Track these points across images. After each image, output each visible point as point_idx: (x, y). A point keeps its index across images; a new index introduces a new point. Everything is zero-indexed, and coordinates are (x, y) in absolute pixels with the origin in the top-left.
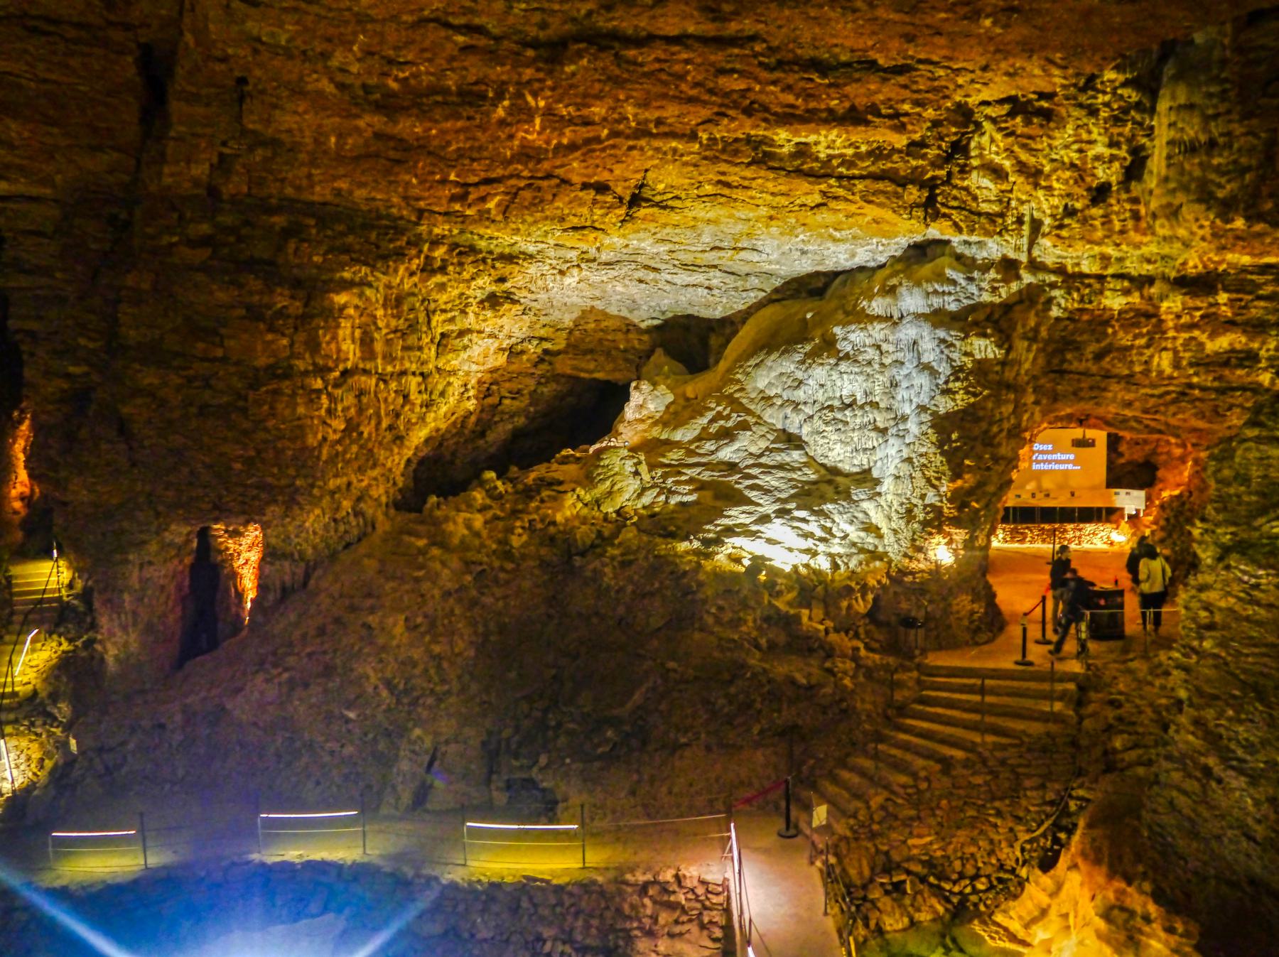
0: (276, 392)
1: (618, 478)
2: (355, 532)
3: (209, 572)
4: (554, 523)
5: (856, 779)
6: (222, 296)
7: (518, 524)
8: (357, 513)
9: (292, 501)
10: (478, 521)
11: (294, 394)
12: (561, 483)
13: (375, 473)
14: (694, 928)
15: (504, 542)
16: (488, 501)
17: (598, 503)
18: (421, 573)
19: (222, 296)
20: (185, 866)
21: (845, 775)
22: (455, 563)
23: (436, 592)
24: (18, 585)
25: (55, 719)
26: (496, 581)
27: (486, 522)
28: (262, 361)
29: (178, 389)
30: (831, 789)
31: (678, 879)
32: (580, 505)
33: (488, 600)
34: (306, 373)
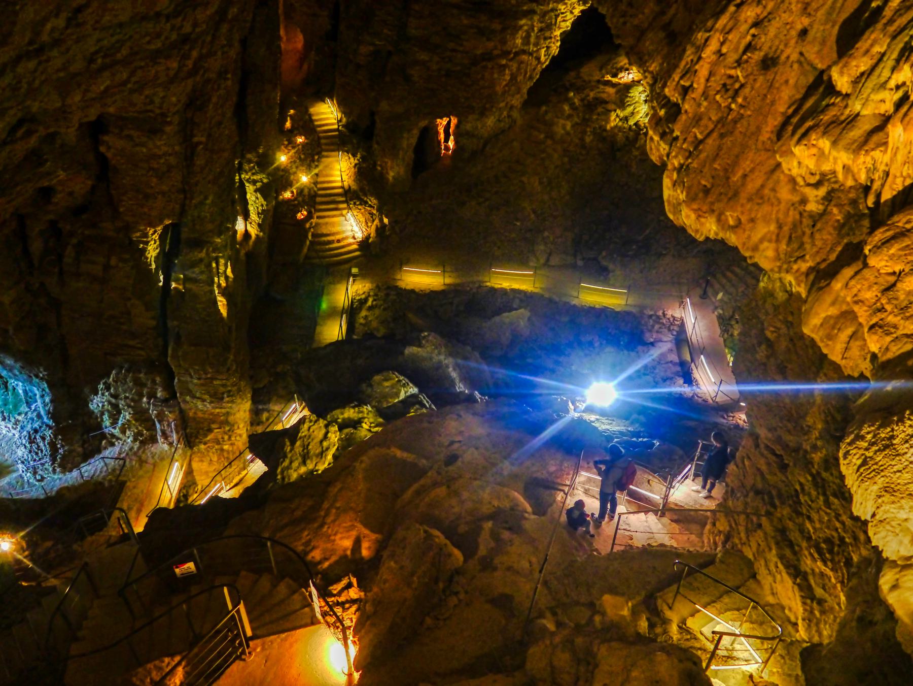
0: (485, 67)
1: (637, 105)
2: (507, 126)
3: (428, 133)
4: (605, 130)
6: (465, 22)
7: (588, 129)
9: (483, 113)
11: (493, 68)
12: (607, 103)
13: (519, 96)
14: (666, 330)
16: (571, 112)
17: (626, 119)
18: (543, 155)
19: (465, 22)
20: (458, 285)
21: (729, 274)
23: (553, 167)
24: (317, 120)
25: (366, 203)
27: (573, 126)
28: (479, 52)
31: (664, 315)
32: (618, 120)
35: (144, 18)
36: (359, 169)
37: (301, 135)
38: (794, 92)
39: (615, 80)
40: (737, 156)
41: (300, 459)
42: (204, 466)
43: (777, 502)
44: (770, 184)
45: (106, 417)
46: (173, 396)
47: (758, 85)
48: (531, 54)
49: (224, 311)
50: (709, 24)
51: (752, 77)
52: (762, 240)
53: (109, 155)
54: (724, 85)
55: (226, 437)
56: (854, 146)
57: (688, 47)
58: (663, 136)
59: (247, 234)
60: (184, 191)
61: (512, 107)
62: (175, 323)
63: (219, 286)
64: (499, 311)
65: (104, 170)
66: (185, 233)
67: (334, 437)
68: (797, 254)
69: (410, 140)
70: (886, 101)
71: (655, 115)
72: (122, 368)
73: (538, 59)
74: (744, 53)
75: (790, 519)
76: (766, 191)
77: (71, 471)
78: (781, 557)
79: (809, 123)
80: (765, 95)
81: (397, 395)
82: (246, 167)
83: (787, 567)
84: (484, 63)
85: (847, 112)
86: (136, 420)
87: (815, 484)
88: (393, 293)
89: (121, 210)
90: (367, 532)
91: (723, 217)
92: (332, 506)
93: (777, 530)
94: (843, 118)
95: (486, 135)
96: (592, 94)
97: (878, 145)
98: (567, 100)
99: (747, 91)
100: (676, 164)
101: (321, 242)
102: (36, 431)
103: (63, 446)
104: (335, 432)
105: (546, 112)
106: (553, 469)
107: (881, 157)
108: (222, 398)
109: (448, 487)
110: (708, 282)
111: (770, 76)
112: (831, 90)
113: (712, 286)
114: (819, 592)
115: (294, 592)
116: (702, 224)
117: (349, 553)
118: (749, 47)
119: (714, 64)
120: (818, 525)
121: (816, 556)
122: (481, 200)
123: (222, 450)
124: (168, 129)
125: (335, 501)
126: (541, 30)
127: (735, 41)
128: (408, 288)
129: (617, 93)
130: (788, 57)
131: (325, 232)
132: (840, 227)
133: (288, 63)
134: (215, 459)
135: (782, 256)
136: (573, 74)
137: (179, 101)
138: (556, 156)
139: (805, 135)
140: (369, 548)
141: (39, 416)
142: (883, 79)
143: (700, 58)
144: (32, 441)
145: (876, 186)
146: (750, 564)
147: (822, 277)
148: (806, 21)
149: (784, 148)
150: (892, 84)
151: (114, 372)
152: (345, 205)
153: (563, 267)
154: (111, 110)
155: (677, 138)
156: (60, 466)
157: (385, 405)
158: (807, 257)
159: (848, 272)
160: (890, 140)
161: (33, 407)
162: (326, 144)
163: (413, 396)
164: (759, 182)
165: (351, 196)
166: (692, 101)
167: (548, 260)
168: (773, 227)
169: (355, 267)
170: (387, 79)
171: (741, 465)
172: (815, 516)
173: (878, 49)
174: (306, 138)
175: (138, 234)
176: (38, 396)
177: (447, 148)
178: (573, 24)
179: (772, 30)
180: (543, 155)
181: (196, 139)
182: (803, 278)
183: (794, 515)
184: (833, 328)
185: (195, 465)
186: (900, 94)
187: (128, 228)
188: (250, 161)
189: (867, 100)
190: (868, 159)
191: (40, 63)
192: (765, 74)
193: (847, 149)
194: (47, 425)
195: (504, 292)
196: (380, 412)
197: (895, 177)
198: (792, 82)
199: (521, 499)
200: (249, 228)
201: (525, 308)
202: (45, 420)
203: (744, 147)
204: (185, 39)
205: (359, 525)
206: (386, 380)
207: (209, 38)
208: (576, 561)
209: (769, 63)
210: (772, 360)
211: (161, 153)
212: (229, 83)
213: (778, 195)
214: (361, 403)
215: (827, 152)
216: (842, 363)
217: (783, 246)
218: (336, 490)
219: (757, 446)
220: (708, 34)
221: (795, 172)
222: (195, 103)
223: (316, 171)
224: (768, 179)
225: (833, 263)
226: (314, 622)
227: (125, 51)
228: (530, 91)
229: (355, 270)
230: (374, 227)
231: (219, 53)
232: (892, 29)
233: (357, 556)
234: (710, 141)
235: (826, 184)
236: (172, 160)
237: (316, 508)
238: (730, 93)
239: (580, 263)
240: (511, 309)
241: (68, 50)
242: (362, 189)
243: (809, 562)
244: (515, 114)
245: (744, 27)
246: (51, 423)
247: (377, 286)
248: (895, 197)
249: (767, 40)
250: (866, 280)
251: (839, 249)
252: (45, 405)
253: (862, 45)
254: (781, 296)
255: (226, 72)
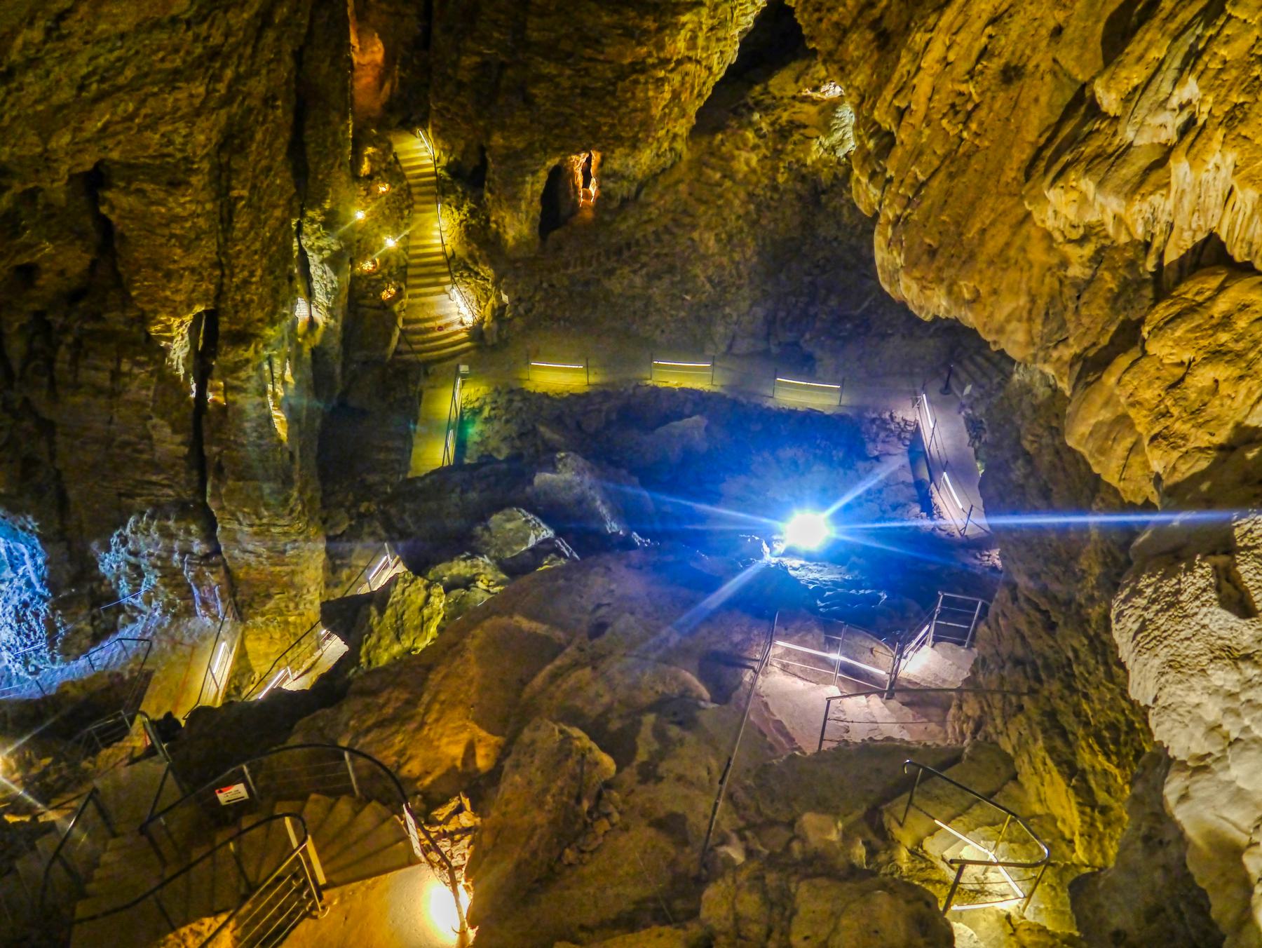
0: (636, 82)
3: (559, 176)
4: (805, 165)
5: (986, 364)
6: (606, 19)
8: (671, 149)
9: (635, 146)
10: (754, 160)
11: (646, 83)
12: (805, 127)
13: (683, 121)
14: (895, 439)
15: (774, 179)
16: (757, 141)
17: (833, 149)
18: (720, 202)
19: (606, 19)
20: (607, 384)
22: (742, 195)
25: (477, 274)
26: (768, 207)
28: (627, 61)
29: (569, 78)
30: (972, 368)
31: (892, 418)
33: (764, 222)
34: (654, 66)
35: (157, 25)
36: (467, 227)
37: (384, 181)
38: (1046, 114)
39: (816, 95)
40: (972, 205)
41: (392, 634)
42: (262, 647)
43: (1044, 676)
44: (1018, 241)
45: (123, 582)
46: (217, 551)
47: (997, 105)
48: (698, 62)
49: (282, 431)
50: (931, 20)
51: (989, 94)
52: (1008, 320)
53: (113, 218)
54: (953, 106)
55: (292, 605)
56: (1126, 189)
57: (903, 53)
58: (873, 176)
59: (312, 324)
60: (219, 265)
61: (675, 136)
62: (215, 449)
63: (275, 396)
64: (666, 419)
65: (107, 238)
66: (224, 325)
67: (439, 601)
68: (1057, 337)
69: (535, 185)
70: (1166, 126)
71: (861, 147)
72: (142, 513)
73: (709, 69)
74: (978, 61)
75: (1062, 698)
76: (1012, 253)
77: (77, 659)
78: (1051, 750)
79: (1067, 157)
80: (1008, 119)
81: (525, 540)
82: (307, 228)
83: (1058, 764)
84: (634, 77)
85: (1117, 141)
86: (165, 585)
87: (1094, 651)
88: (517, 398)
89: (134, 293)
90: (483, 734)
91: (956, 288)
92: (434, 699)
93: (1044, 713)
94: (1110, 150)
95: (640, 176)
96: (785, 116)
97: (1159, 187)
98: (751, 124)
99: (982, 113)
100: (891, 216)
101: (415, 330)
102: (25, 605)
103: (64, 625)
104: (439, 595)
105: (722, 143)
106: (737, 638)
107: (1162, 203)
108: (284, 552)
109: (594, 668)
110: (950, 371)
111: (1013, 92)
112: (1095, 111)
113: (956, 376)
114: (1102, 797)
115: (384, 821)
116: (928, 299)
117: (459, 763)
118: (984, 53)
119: (938, 76)
120: (1098, 707)
121: (1096, 747)
122: (637, 266)
123: (287, 623)
124: (194, 180)
125: (438, 693)
126: (712, 29)
127: (966, 44)
128: (539, 390)
129: (820, 113)
130: (1037, 66)
131: (421, 316)
132: (1114, 299)
133: (364, 81)
134: (277, 636)
135: (1037, 340)
136: (758, 88)
137: (209, 139)
138: (737, 202)
139: (1061, 173)
140: (487, 756)
141: (29, 584)
142: (1162, 97)
143: (919, 68)
144: (20, 619)
145: (1157, 243)
146: (1009, 760)
147: (1091, 367)
148: (1060, 16)
149: (1033, 192)
150: (1174, 102)
151: (132, 520)
152: (448, 279)
153: (751, 355)
154: (115, 155)
155: (890, 181)
156: (61, 652)
157: (508, 555)
158: (1071, 341)
159: (1123, 361)
160: (1173, 180)
161: (20, 572)
162: (421, 194)
163: (546, 541)
164: (1001, 240)
165: (456, 266)
166: (910, 129)
167: (730, 347)
168: (1023, 300)
169: (464, 363)
170: (501, 101)
171: (994, 626)
172: (1092, 692)
173: (1155, 54)
174: (392, 186)
175: (158, 327)
176: (26, 557)
177: (587, 196)
178: (756, 20)
179: (1016, 26)
180: (720, 202)
181: (235, 193)
182: (1066, 369)
183: (1066, 693)
184: (1107, 438)
185: (249, 645)
186: (1185, 116)
187: (144, 319)
188: (313, 221)
189: (1142, 124)
190: (1146, 206)
191: (9, 93)
192: (1006, 90)
193: (1117, 193)
194: (41, 596)
195: (671, 393)
196: (502, 565)
197: (1182, 230)
198: (1044, 99)
199: (695, 681)
200: (314, 313)
201: (701, 413)
202: (38, 589)
203: (982, 191)
204: (214, 54)
205: (471, 725)
206: (509, 520)
207: (249, 51)
208: (772, 765)
209: (1011, 74)
210: (1032, 480)
211: (185, 214)
212: (279, 112)
213: (1030, 256)
214: (475, 553)
215: (1091, 197)
216: (1120, 486)
217: (1038, 327)
218: (439, 677)
219: (1015, 599)
220: (929, 36)
221: (1050, 224)
222: (232, 141)
223: (407, 232)
224: (1014, 234)
225: (1105, 348)
226: (412, 861)
227: (129, 73)
228: (699, 114)
229: (464, 368)
230: (489, 307)
231: (264, 72)
232: (1173, 26)
233: (470, 769)
234: (935, 183)
235: (1094, 239)
236: (201, 222)
237: (412, 703)
238: (961, 117)
239: (775, 350)
240: (680, 417)
241: (48, 73)
242: (471, 256)
243: (1087, 756)
244: (680, 145)
245: (979, 24)
246: (46, 593)
247: (496, 390)
248: (1182, 257)
249: (1008, 44)
250: (1146, 372)
251: (1113, 328)
252: (37, 567)
253: (1135, 48)
254: (1042, 392)
255: (275, 98)
